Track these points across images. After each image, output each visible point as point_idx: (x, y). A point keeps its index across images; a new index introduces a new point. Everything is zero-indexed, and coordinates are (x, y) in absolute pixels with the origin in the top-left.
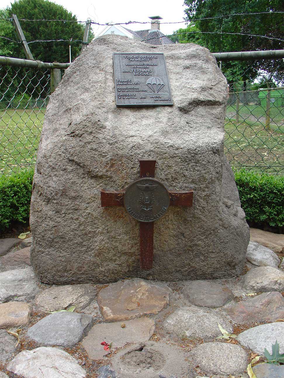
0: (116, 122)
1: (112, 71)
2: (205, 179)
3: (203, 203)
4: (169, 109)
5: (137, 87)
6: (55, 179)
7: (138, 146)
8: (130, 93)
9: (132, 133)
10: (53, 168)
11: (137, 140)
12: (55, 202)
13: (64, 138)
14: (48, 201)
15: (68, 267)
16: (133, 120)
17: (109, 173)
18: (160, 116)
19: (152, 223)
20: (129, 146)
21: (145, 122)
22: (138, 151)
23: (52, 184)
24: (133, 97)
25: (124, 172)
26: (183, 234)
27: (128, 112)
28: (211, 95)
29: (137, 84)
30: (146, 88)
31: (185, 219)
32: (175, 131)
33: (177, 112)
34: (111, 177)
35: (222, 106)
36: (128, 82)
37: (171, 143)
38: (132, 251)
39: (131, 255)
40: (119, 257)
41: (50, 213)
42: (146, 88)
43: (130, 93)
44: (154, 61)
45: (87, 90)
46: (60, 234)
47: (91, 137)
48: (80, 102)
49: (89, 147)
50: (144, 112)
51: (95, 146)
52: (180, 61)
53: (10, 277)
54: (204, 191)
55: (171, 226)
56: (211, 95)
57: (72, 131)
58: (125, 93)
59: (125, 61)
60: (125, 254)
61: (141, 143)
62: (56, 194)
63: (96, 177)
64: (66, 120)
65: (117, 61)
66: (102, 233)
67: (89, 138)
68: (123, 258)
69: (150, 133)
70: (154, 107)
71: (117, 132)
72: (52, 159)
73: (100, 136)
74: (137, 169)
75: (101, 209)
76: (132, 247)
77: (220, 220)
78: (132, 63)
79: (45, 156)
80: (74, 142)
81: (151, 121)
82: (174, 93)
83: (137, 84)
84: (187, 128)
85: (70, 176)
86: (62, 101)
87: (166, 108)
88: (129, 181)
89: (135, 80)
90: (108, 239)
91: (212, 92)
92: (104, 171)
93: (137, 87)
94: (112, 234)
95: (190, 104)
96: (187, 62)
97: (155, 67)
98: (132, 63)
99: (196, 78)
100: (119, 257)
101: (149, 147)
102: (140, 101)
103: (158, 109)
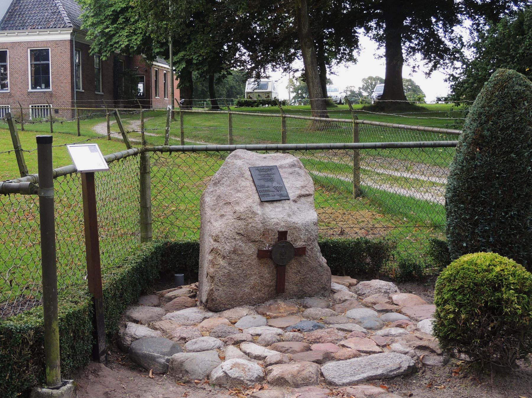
0: (263, 211)
1: (252, 179)
2: (310, 239)
3: (309, 253)
4: (288, 202)
5: (269, 189)
6: (228, 244)
7: (277, 224)
8: (266, 193)
9: (273, 217)
10: (227, 238)
11: (276, 220)
12: (228, 258)
13: (233, 221)
14: (224, 257)
15: (235, 297)
16: (271, 209)
17: (262, 239)
18: (284, 206)
19: (285, 265)
20: (273, 224)
21: (277, 210)
22: (277, 226)
23: (226, 247)
24: (268, 195)
25: (270, 238)
26: (299, 271)
27: (267, 204)
28: (307, 190)
29: (268, 187)
30: (273, 189)
31: (301, 263)
32: (294, 214)
33: (292, 203)
34: (263, 242)
35: (313, 196)
36: (263, 186)
37: (293, 221)
38: (271, 284)
39: (269, 286)
40: (264, 289)
41: (225, 265)
42: (273, 189)
43: (266, 193)
44: (273, 171)
45: (238, 191)
46: (231, 277)
47: (252, 220)
48: (237, 199)
49: (250, 225)
50: (275, 204)
51: (254, 225)
52: (286, 170)
53: (191, 311)
54: (310, 246)
55: (293, 267)
56: (307, 190)
57: (238, 216)
58: (264, 193)
59: (257, 172)
60: (268, 286)
61: (278, 221)
62: (229, 254)
63: (254, 241)
64: (228, 210)
65: (252, 172)
66: (255, 274)
67: (250, 221)
68: (266, 289)
69: (282, 216)
70: (280, 200)
71: (265, 216)
72: (226, 233)
73: (257, 219)
74: (277, 236)
75: (256, 260)
76: (272, 281)
77: (319, 262)
78: (261, 173)
79: (221, 232)
80: (240, 223)
81: (281, 209)
82: (289, 191)
83: (268, 187)
84: (299, 212)
85: (238, 242)
86: (219, 196)
87: (287, 201)
88: (272, 242)
89: (267, 184)
90: (259, 277)
91: (307, 188)
92: (259, 238)
93: (269, 189)
94: (261, 274)
95: (298, 197)
96: (290, 170)
97: (274, 175)
98: (261, 173)
99: (297, 180)
100: (264, 289)
101: (283, 224)
102: (272, 197)
103: (283, 202)
